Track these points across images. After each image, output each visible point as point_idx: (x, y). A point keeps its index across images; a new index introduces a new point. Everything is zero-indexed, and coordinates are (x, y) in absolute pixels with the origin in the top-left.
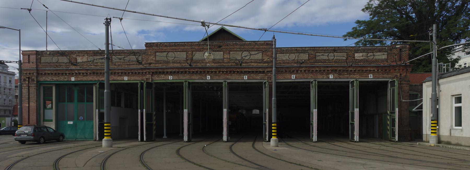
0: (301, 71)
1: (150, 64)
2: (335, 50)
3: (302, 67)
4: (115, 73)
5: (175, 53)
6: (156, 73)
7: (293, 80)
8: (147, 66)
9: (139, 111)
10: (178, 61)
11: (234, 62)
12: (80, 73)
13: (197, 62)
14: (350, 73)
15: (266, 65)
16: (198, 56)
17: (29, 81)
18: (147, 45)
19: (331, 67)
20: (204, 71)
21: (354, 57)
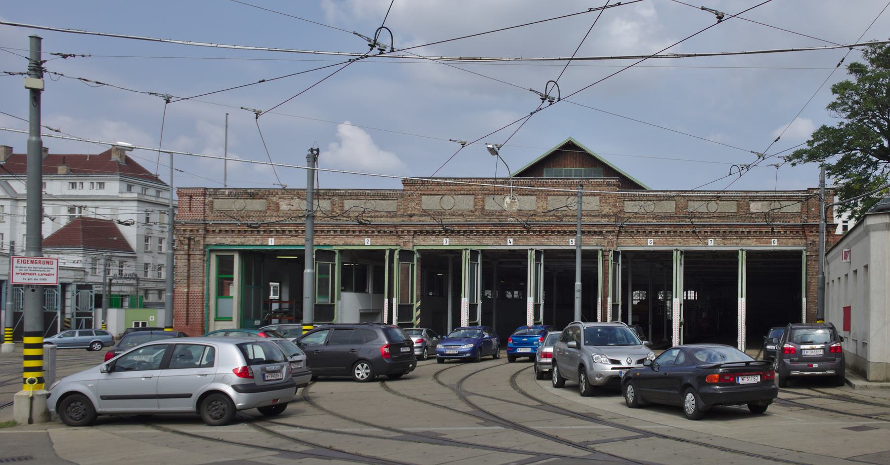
0: (663, 232)
1: (411, 216)
2: (718, 197)
3: (664, 226)
4: (348, 231)
5: (455, 197)
6: (421, 232)
7: (652, 249)
8: (406, 220)
9: (386, 301)
10: (460, 212)
11: (554, 215)
12: (284, 231)
13: (491, 213)
14: (741, 236)
15: (604, 221)
16: (491, 204)
17: (189, 245)
18: (405, 182)
19: (710, 226)
20: (501, 229)
21: (749, 210)
